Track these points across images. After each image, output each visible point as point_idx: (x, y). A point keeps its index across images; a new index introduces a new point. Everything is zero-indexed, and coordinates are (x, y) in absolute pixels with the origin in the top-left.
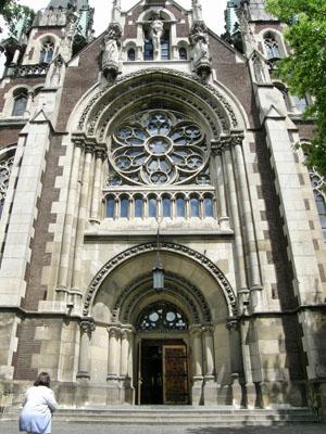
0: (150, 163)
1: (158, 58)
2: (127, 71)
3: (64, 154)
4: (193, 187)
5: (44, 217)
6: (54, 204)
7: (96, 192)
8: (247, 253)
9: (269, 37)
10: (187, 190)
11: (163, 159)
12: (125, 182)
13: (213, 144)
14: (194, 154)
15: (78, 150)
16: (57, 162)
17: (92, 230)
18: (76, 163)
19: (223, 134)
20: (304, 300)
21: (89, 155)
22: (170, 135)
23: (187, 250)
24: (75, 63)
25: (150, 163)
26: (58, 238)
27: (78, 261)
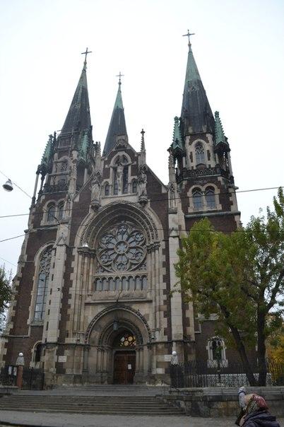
0: (117, 258)
1: (120, 194)
2: (105, 203)
3: (74, 260)
4: (137, 272)
5: (66, 296)
6: (70, 289)
7: (90, 278)
8: (155, 312)
9: (199, 145)
10: (134, 274)
11: (123, 254)
12: (105, 270)
13: (148, 247)
14: (141, 251)
15: (81, 257)
16: (70, 265)
17: (89, 300)
18: (80, 265)
19: (152, 243)
20: (173, 338)
21: (86, 259)
22: (127, 240)
23: (131, 309)
24: (77, 200)
25: (117, 258)
26: (72, 307)
27: (82, 316)
